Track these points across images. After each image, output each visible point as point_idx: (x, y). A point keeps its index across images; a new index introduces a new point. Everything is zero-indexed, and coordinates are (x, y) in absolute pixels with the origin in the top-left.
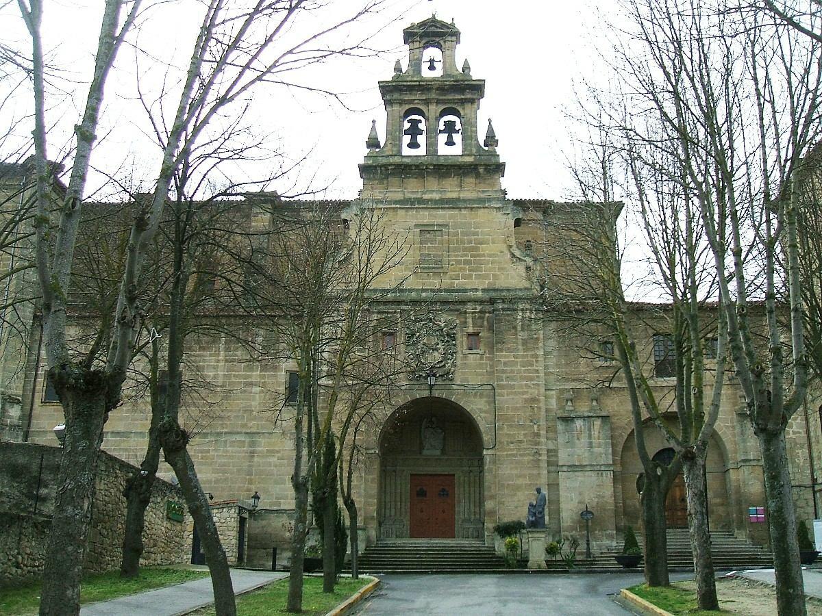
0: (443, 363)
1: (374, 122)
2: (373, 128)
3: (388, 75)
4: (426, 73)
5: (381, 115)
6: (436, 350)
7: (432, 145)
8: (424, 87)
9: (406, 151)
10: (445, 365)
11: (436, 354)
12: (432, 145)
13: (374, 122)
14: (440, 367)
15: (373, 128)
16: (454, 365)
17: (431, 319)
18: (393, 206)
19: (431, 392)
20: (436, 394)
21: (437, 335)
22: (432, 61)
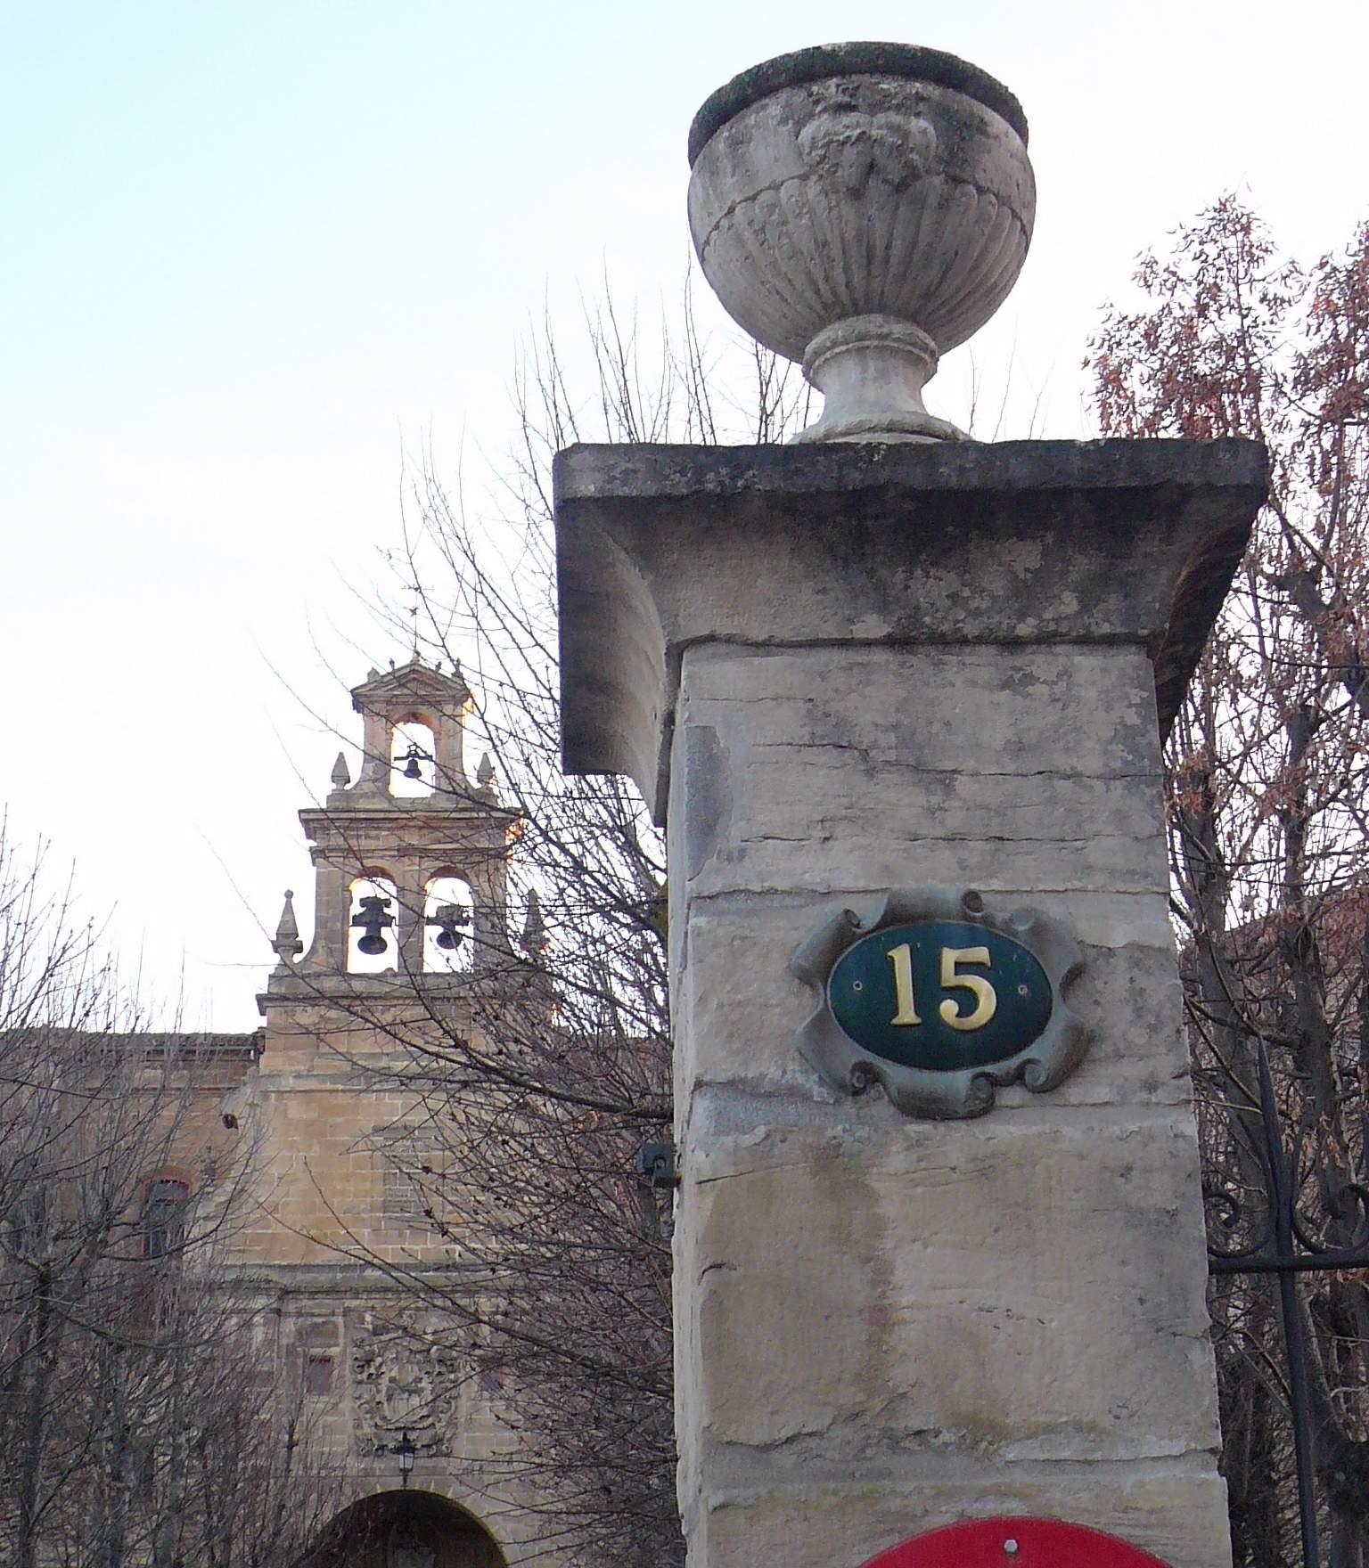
0: (430, 1420)
1: (289, 895)
2: (288, 909)
3: (320, 793)
4: (402, 787)
5: (303, 878)
6: (418, 1392)
7: (411, 952)
8: (401, 817)
9: (360, 962)
10: (433, 1425)
11: (415, 1400)
12: (411, 952)
13: (289, 895)
14: (424, 1428)
15: (288, 909)
16: (452, 1423)
17: (405, 1329)
18: (329, 1086)
19: (405, 1481)
20: (416, 1484)
21: (418, 1363)
22: (413, 757)
